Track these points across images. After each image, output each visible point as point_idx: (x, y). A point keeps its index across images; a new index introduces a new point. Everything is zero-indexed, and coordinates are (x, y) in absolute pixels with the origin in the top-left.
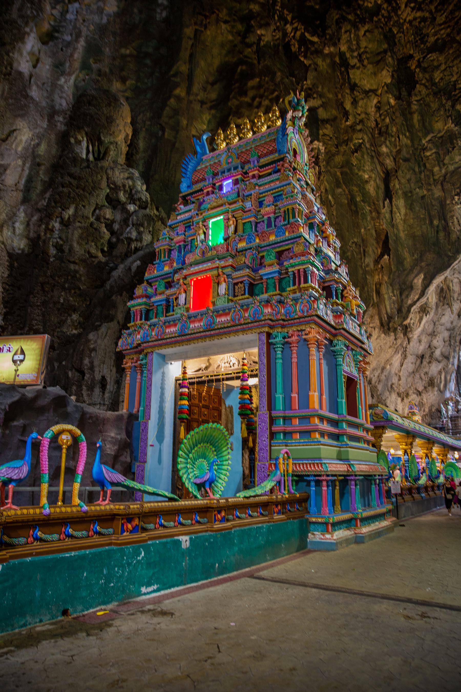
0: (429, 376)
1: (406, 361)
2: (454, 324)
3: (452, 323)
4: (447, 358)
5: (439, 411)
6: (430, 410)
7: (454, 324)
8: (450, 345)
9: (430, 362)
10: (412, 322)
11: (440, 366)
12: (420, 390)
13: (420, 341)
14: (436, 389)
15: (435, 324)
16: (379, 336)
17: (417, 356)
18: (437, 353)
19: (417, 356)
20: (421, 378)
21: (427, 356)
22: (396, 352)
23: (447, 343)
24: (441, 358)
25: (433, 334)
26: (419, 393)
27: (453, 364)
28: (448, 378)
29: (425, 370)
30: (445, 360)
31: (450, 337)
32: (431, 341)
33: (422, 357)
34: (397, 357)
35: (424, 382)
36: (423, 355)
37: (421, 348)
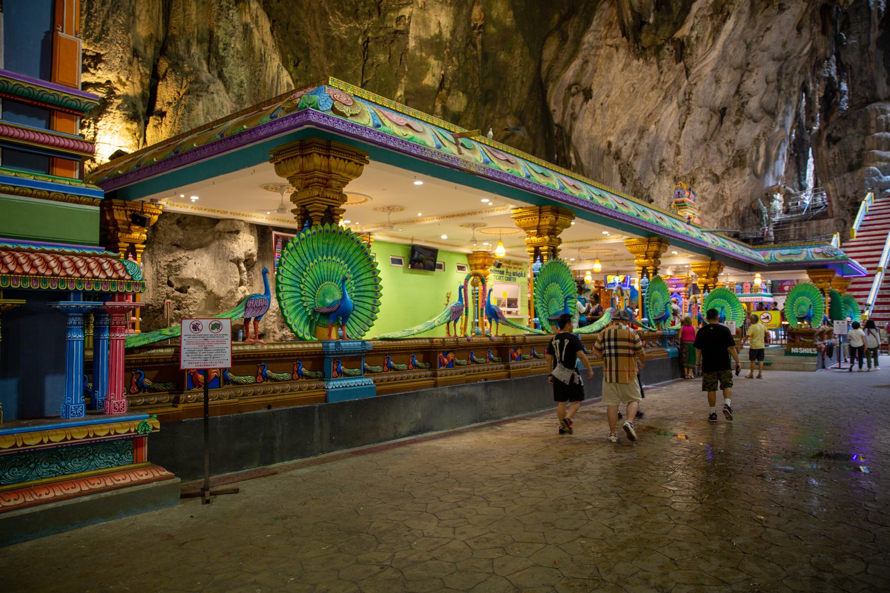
0: (736, 147)
1: (689, 119)
2: (789, 47)
3: (784, 45)
4: (772, 114)
5: (758, 213)
6: (736, 209)
7: (789, 47)
8: (779, 90)
9: (738, 122)
10: (694, 34)
11: (758, 129)
12: (718, 172)
13: (718, 81)
14: (748, 170)
15: (748, 47)
16: (626, 66)
17: (712, 110)
18: (753, 104)
19: (712, 110)
20: (720, 151)
21: (733, 110)
22: (666, 98)
23: (772, 86)
24: (759, 115)
25: (745, 69)
26: (716, 179)
27: (783, 126)
28: (774, 152)
29: (728, 137)
30: (767, 117)
31: (779, 73)
32: (742, 82)
33: (723, 112)
34: (670, 109)
35: (726, 159)
36: (725, 109)
37: (722, 94)
